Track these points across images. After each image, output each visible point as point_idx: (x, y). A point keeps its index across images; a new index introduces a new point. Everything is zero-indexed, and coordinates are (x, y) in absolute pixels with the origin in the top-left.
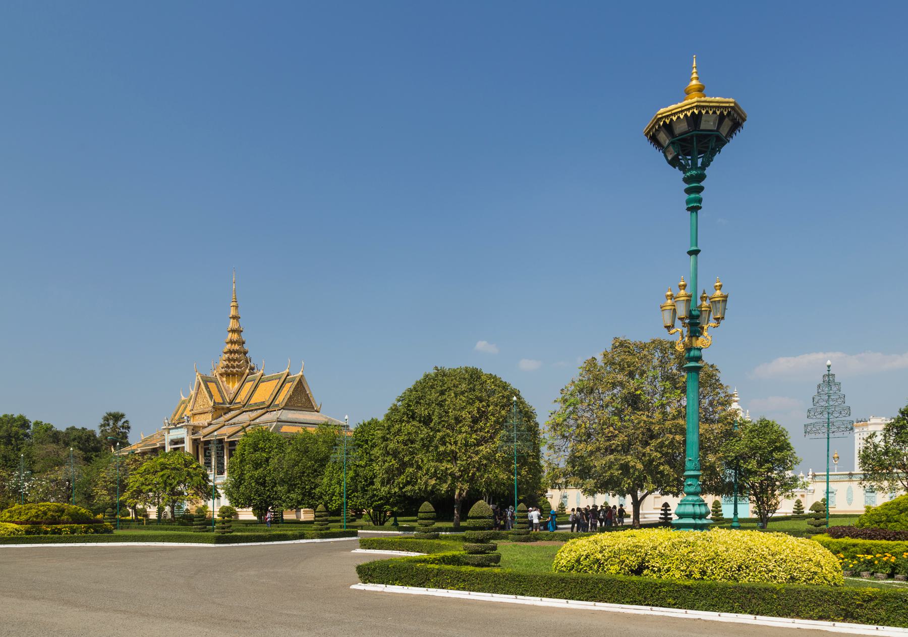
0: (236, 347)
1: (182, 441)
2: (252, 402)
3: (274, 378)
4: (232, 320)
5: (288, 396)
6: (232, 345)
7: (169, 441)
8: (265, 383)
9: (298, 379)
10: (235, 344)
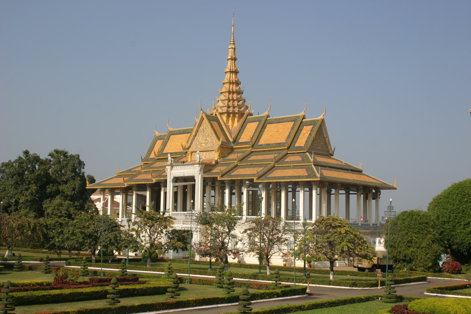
0: (235, 88)
1: (192, 179)
2: (262, 141)
3: (285, 120)
4: (230, 61)
5: (311, 139)
6: (230, 85)
7: (172, 177)
8: (275, 124)
9: (320, 122)
10: (233, 85)
